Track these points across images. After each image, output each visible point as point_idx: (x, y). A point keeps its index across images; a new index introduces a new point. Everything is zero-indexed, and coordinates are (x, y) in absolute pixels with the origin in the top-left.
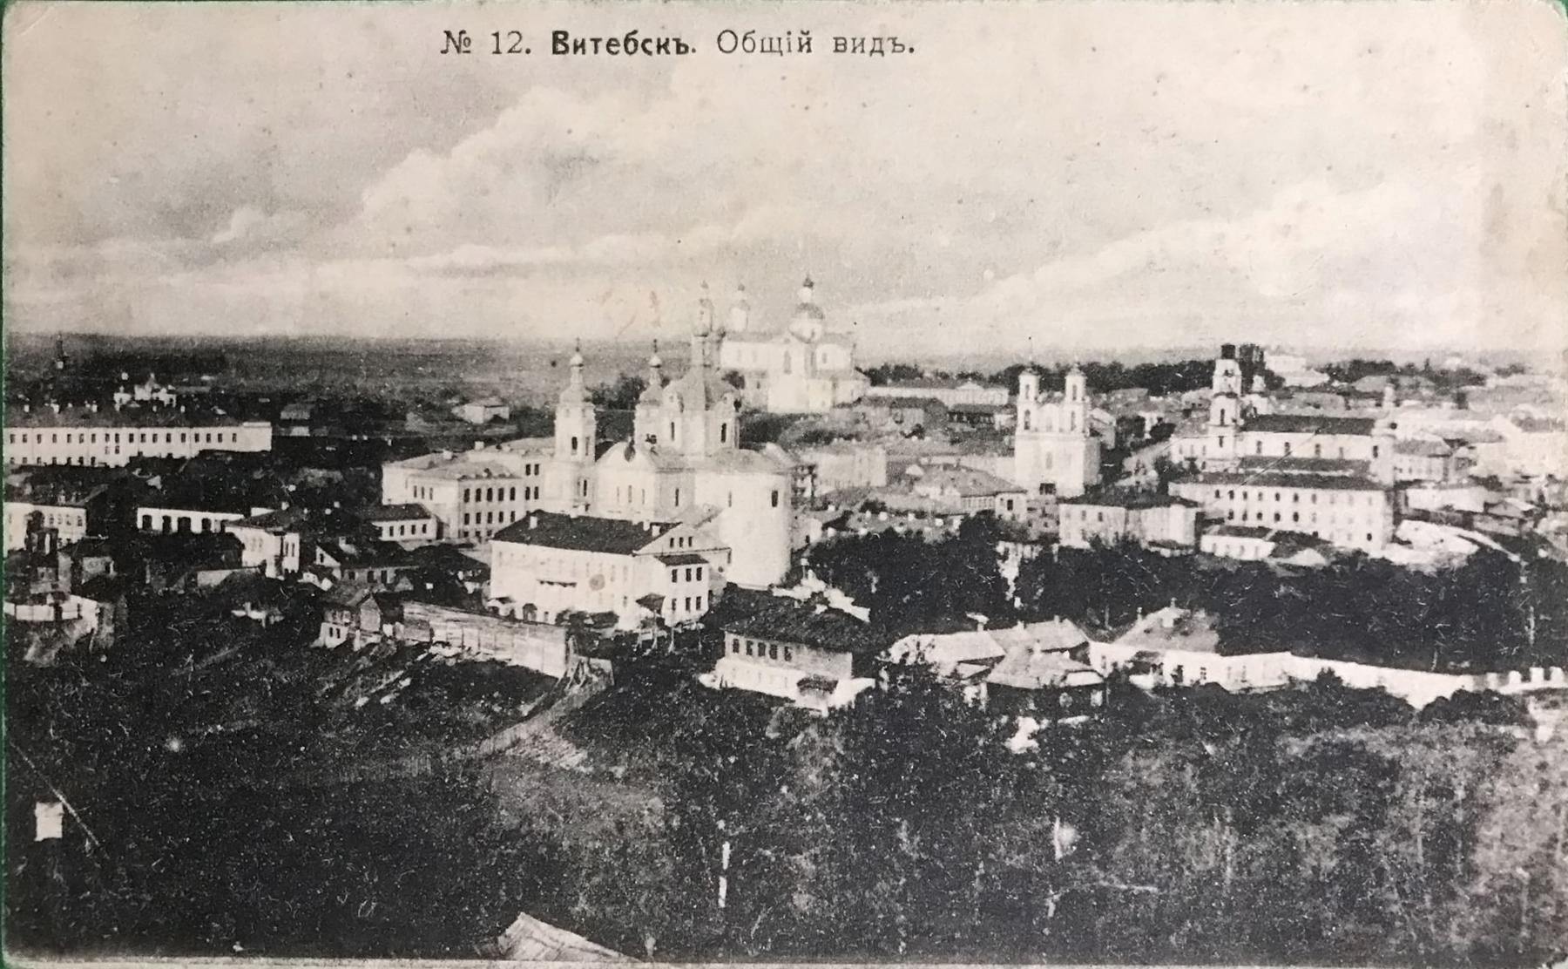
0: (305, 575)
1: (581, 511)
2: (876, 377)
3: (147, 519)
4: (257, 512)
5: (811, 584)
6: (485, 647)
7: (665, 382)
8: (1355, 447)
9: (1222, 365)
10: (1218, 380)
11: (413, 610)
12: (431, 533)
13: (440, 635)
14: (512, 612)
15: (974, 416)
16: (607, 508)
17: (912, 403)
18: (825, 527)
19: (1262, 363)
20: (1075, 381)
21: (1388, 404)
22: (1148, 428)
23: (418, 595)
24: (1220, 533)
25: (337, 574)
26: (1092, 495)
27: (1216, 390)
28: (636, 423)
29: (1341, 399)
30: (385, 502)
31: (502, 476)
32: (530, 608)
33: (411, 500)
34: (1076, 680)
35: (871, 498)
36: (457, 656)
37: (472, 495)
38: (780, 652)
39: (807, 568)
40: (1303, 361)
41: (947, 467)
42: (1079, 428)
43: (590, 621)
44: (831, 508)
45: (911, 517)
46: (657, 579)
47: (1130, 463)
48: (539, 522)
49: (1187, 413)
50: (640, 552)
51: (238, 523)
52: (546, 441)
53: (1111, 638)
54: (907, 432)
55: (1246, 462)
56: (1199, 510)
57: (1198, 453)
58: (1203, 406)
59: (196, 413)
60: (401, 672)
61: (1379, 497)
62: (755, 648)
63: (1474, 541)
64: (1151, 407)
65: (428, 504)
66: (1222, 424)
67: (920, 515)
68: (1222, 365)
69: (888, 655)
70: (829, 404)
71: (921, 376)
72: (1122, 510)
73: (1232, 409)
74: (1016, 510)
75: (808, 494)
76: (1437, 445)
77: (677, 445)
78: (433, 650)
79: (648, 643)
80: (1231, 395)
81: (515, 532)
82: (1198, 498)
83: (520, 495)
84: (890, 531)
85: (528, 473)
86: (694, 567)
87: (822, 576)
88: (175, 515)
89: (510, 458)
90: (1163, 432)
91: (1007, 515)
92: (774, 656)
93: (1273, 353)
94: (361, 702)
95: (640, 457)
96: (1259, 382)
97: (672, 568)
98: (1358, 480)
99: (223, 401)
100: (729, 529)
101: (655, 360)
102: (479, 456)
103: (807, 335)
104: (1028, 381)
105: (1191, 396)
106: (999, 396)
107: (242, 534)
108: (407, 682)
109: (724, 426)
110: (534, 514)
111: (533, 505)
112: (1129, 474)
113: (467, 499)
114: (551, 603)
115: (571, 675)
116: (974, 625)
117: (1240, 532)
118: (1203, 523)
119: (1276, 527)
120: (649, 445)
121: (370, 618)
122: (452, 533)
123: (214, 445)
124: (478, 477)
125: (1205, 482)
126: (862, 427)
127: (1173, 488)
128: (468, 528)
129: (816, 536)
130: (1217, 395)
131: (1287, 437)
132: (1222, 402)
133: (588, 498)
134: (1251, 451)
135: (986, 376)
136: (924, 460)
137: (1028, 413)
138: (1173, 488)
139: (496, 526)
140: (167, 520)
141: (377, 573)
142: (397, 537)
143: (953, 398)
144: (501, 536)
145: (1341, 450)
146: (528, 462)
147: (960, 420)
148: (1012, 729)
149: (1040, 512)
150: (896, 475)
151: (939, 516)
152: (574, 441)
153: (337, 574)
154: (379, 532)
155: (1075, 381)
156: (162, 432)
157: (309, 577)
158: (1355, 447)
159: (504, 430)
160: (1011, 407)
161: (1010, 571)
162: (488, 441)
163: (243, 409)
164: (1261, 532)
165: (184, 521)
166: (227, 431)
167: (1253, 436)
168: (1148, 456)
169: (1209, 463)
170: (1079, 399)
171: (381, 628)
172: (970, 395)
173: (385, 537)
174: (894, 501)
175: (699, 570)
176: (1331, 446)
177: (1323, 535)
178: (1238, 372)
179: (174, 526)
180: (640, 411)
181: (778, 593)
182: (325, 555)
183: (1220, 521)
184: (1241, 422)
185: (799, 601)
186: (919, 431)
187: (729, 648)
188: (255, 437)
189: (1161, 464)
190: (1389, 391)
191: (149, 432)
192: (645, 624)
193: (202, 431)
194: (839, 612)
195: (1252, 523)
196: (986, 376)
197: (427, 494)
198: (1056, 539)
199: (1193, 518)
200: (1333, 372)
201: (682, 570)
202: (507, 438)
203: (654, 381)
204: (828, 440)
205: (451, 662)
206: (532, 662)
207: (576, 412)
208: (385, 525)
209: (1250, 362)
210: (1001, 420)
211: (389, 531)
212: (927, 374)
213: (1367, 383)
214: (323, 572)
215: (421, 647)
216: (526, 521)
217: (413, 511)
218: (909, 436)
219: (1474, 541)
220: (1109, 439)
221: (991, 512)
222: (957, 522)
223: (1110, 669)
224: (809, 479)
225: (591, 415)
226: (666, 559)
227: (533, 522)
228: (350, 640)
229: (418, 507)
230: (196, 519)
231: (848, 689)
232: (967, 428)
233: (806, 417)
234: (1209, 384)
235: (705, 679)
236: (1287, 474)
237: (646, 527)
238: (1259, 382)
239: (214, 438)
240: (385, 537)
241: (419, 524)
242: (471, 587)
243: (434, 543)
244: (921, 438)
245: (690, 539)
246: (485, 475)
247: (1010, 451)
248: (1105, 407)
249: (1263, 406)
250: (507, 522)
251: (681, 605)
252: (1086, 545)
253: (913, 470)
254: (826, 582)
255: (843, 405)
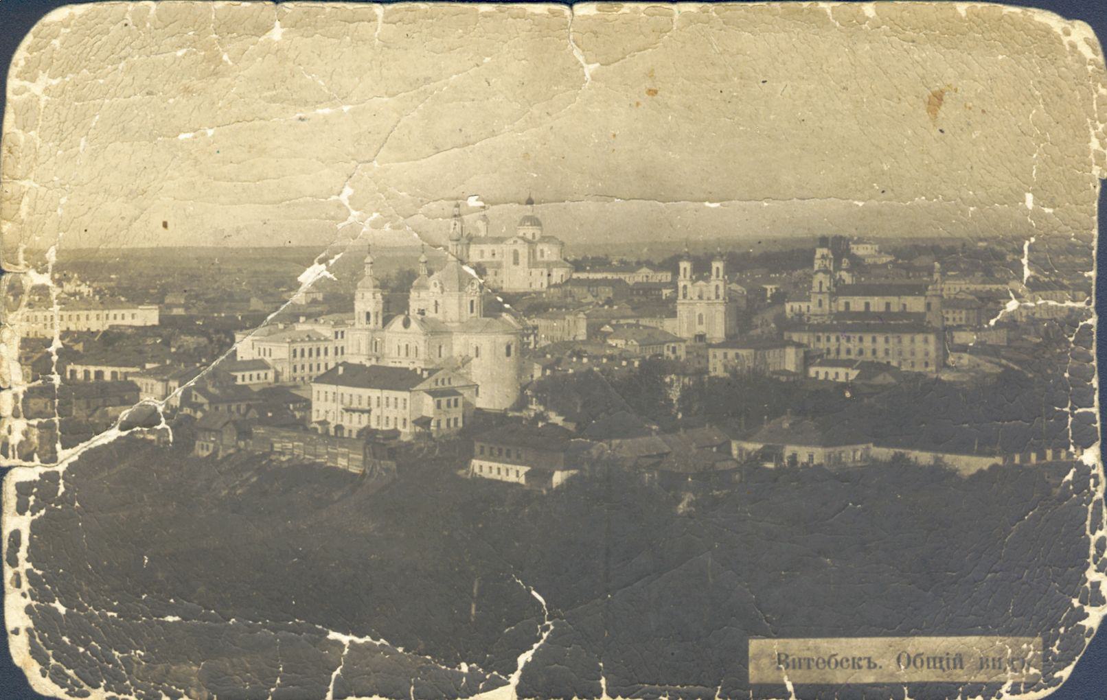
0: (185, 409)
1: (374, 362)
2: (578, 266)
3: (73, 372)
4: (148, 366)
5: (535, 407)
6: (308, 454)
7: (430, 273)
8: (915, 304)
9: (820, 252)
10: (817, 264)
11: (260, 431)
12: (271, 375)
13: (277, 447)
14: (327, 431)
15: (649, 290)
16: (394, 358)
17: (605, 282)
18: (544, 369)
19: (848, 250)
20: (717, 265)
21: (936, 276)
22: (769, 295)
23: (263, 422)
24: (821, 365)
25: (206, 407)
26: (731, 341)
27: (816, 267)
28: (411, 303)
29: (904, 272)
30: (239, 359)
31: (319, 340)
32: (339, 428)
33: (260, 358)
34: (720, 466)
35: (577, 348)
36: (289, 460)
37: (298, 353)
38: (513, 455)
39: (532, 397)
40: (877, 247)
41: (629, 325)
42: (721, 298)
43: (381, 436)
44: (549, 356)
45: (605, 360)
46: (428, 406)
47: (757, 320)
48: (344, 370)
49: (796, 285)
50: (415, 389)
51: (134, 374)
52: (350, 315)
53: (746, 438)
54: (600, 303)
55: (839, 316)
56: (806, 349)
57: (804, 309)
58: (808, 278)
59: (108, 298)
60: (250, 473)
61: (932, 338)
62: (496, 452)
63: (1001, 365)
64: (771, 282)
65: (268, 359)
66: (821, 292)
67: (611, 358)
68: (820, 252)
69: (589, 453)
70: (545, 285)
71: (610, 263)
72: (752, 351)
73: (827, 283)
74: (678, 353)
75: (532, 346)
76: (972, 301)
77: (440, 316)
78: (273, 457)
79: (421, 450)
80: (826, 271)
81: (330, 377)
82: (805, 341)
83: (331, 351)
84: (590, 371)
85: (336, 337)
86: (453, 399)
87: (541, 401)
88: (92, 369)
89: (324, 329)
90: (780, 298)
91: (672, 357)
92: (508, 455)
93: (856, 243)
94: (224, 493)
95: (414, 325)
96: (845, 263)
97: (436, 400)
98: (917, 324)
99: (125, 291)
100: (478, 371)
101: (423, 259)
102: (303, 327)
103: (529, 236)
104: (685, 265)
105: (799, 272)
106: (666, 277)
107: (139, 381)
108: (254, 479)
109: (472, 302)
110: (341, 365)
111: (340, 359)
112: (757, 327)
113: (295, 356)
114: (354, 423)
115: (368, 472)
116: (649, 433)
117: (835, 363)
118: (808, 359)
119: (860, 359)
120: (419, 317)
121: (229, 438)
122: (286, 376)
123: (119, 322)
124: (303, 341)
125: (809, 331)
126: (569, 300)
127: (786, 335)
128: (295, 375)
129: (537, 374)
130: (817, 272)
131: (868, 299)
132: (820, 276)
133: (378, 354)
134: (842, 308)
135: (656, 262)
136: (614, 322)
137: (685, 287)
138: (785, 338)
139: (315, 373)
140: (87, 373)
141: (234, 408)
142: (247, 381)
143: (630, 279)
144: (320, 379)
145: (905, 305)
146: (337, 329)
147: (638, 294)
148: (679, 501)
149: (695, 354)
150: (594, 331)
151: (625, 359)
152: (368, 315)
153: (206, 407)
154: (235, 378)
155: (717, 265)
156: (83, 313)
157: (187, 411)
158: (915, 304)
159: (319, 309)
160: (673, 285)
161: (675, 394)
162: (309, 316)
163: (136, 296)
164: (848, 364)
165: (99, 374)
166: (127, 313)
167: (842, 301)
168: (769, 315)
169: (813, 318)
170: (721, 278)
171: (237, 443)
172: (642, 275)
173: (239, 382)
174: (589, 349)
175: (456, 401)
176: (896, 303)
177: (894, 363)
178: (831, 256)
179: (92, 376)
180: (413, 294)
181: (510, 414)
182: (199, 395)
183: (821, 356)
184: (834, 289)
185: (526, 419)
186: (609, 302)
187: (477, 450)
188: (148, 316)
189: (781, 320)
190: (937, 265)
191: (74, 314)
192: (418, 436)
193: (112, 313)
194: (555, 425)
195: (843, 356)
196: (656, 262)
197: (267, 353)
198: (707, 372)
199: (802, 354)
200: (897, 252)
201: (444, 401)
202: (320, 314)
203: (423, 271)
204: (546, 310)
205: (286, 465)
206: (342, 463)
207: (369, 295)
208: (239, 375)
209: (839, 246)
210: (666, 292)
211: (241, 379)
212: (614, 263)
213: (924, 260)
214: (197, 407)
215: (264, 455)
216: (336, 368)
217: (259, 365)
218: (603, 306)
219: (1001, 365)
220: (743, 303)
221: (662, 355)
222: (637, 364)
223: (745, 458)
224: (532, 338)
225: (379, 296)
226: (432, 393)
227: (341, 370)
228: (215, 453)
229: (262, 361)
230: (108, 372)
231: (558, 478)
232: (643, 299)
233: (530, 294)
234: (812, 266)
235: (461, 472)
236: (866, 323)
237: (419, 372)
238: (845, 263)
239: (119, 317)
240: (239, 382)
241: (262, 374)
242: (298, 415)
243: (272, 386)
244: (611, 306)
245: (449, 379)
246: (307, 339)
247: (673, 314)
248: (739, 282)
249: (847, 278)
250: (323, 370)
251: (443, 425)
252: (726, 375)
253: (607, 328)
254: (545, 405)
255: (556, 286)
